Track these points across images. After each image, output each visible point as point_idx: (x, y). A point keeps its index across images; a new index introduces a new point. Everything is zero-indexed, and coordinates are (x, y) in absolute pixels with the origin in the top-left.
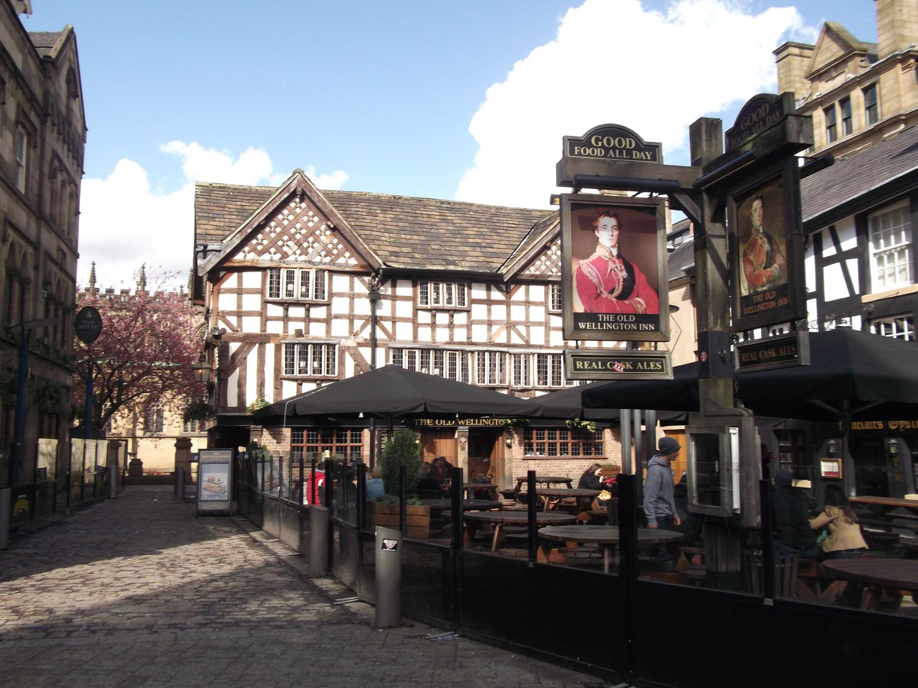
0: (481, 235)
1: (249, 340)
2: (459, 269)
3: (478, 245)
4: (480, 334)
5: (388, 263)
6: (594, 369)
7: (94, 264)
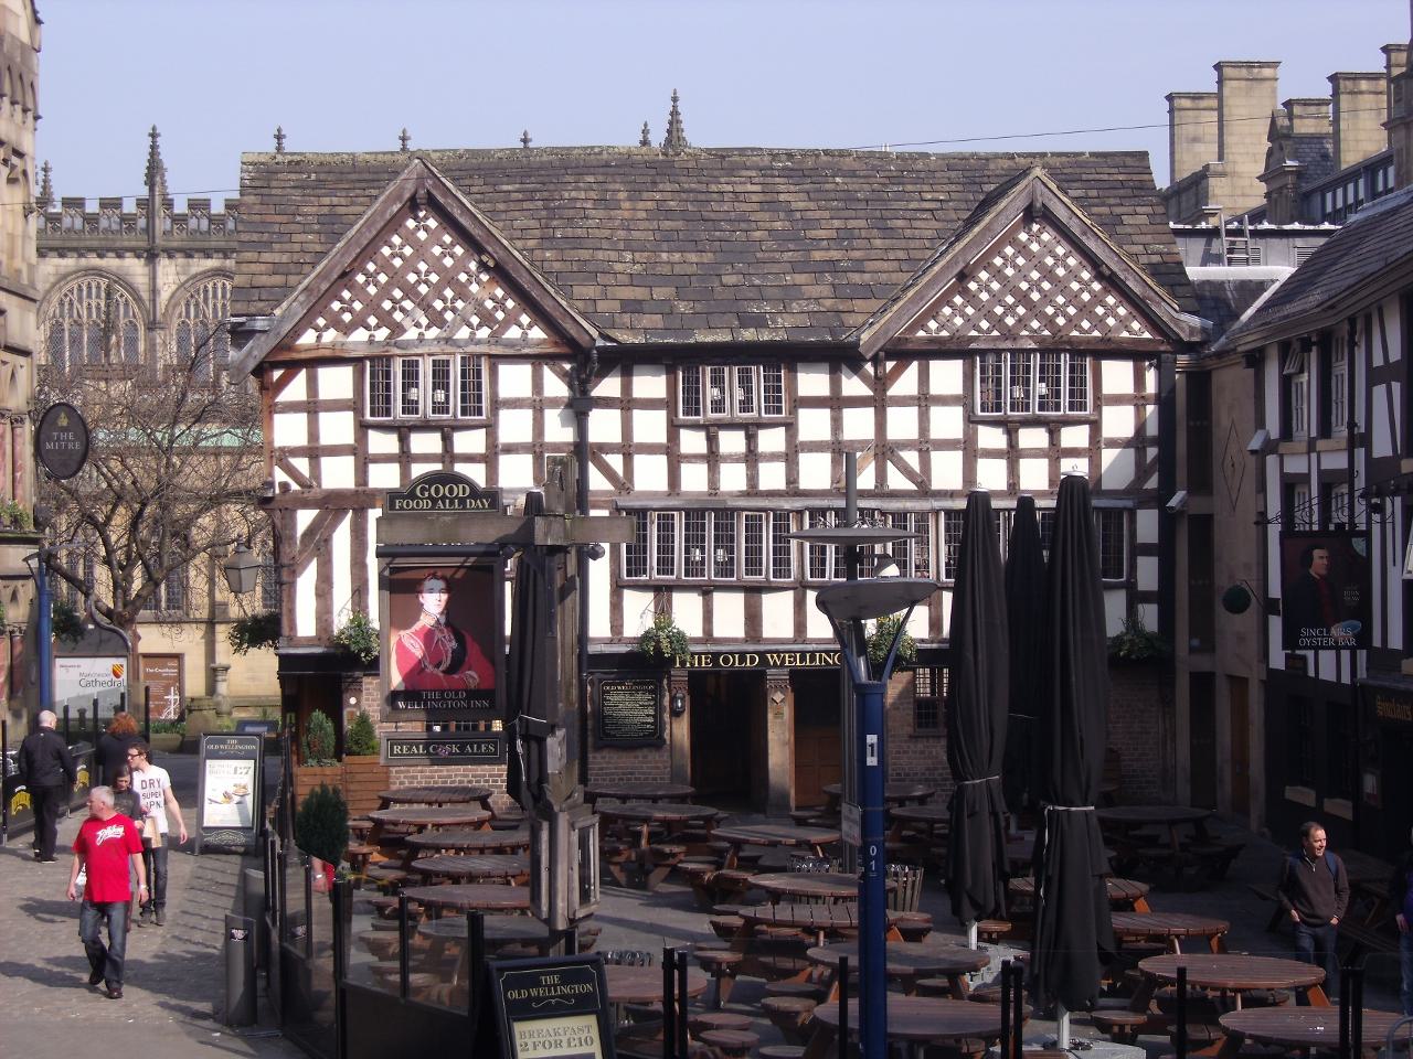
0: (844, 238)
1: (334, 505)
2: (765, 336)
3: (832, 266)
5: (610, 333)
6: (414, 754)
7: (154, 135)
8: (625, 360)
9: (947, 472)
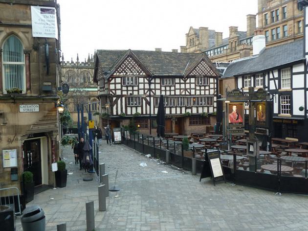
0: (176, 63)
3: (176, 66)
4: (178, 92)
8: (155, 77)
9: (158, 93)
